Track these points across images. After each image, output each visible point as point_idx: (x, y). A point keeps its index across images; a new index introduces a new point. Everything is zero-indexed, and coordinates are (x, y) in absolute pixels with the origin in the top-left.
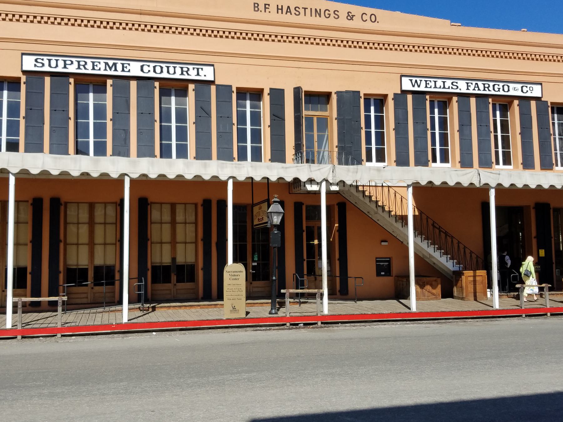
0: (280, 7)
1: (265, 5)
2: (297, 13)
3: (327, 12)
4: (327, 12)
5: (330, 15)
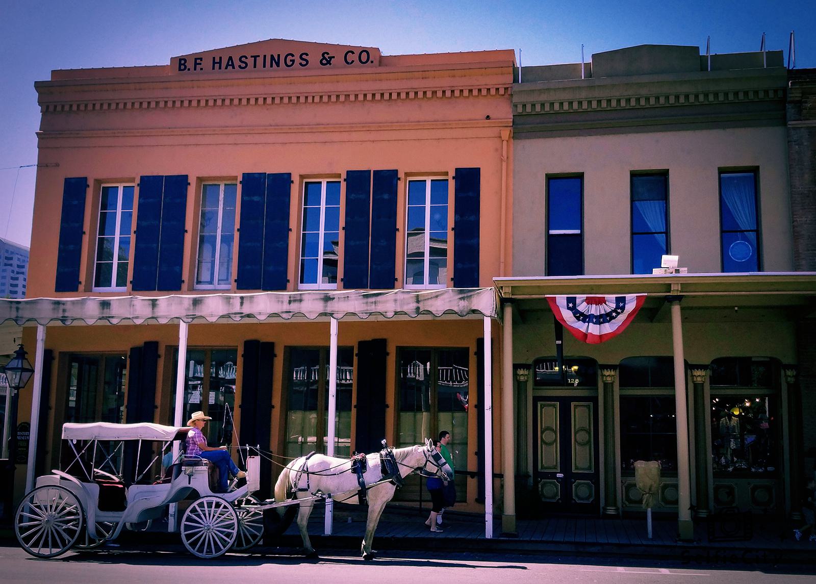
0: (217, 60)
1: (196, 59)
2: (243, 65)
3: (290, 58)
4: (290, 58)
5: (293, 61)
